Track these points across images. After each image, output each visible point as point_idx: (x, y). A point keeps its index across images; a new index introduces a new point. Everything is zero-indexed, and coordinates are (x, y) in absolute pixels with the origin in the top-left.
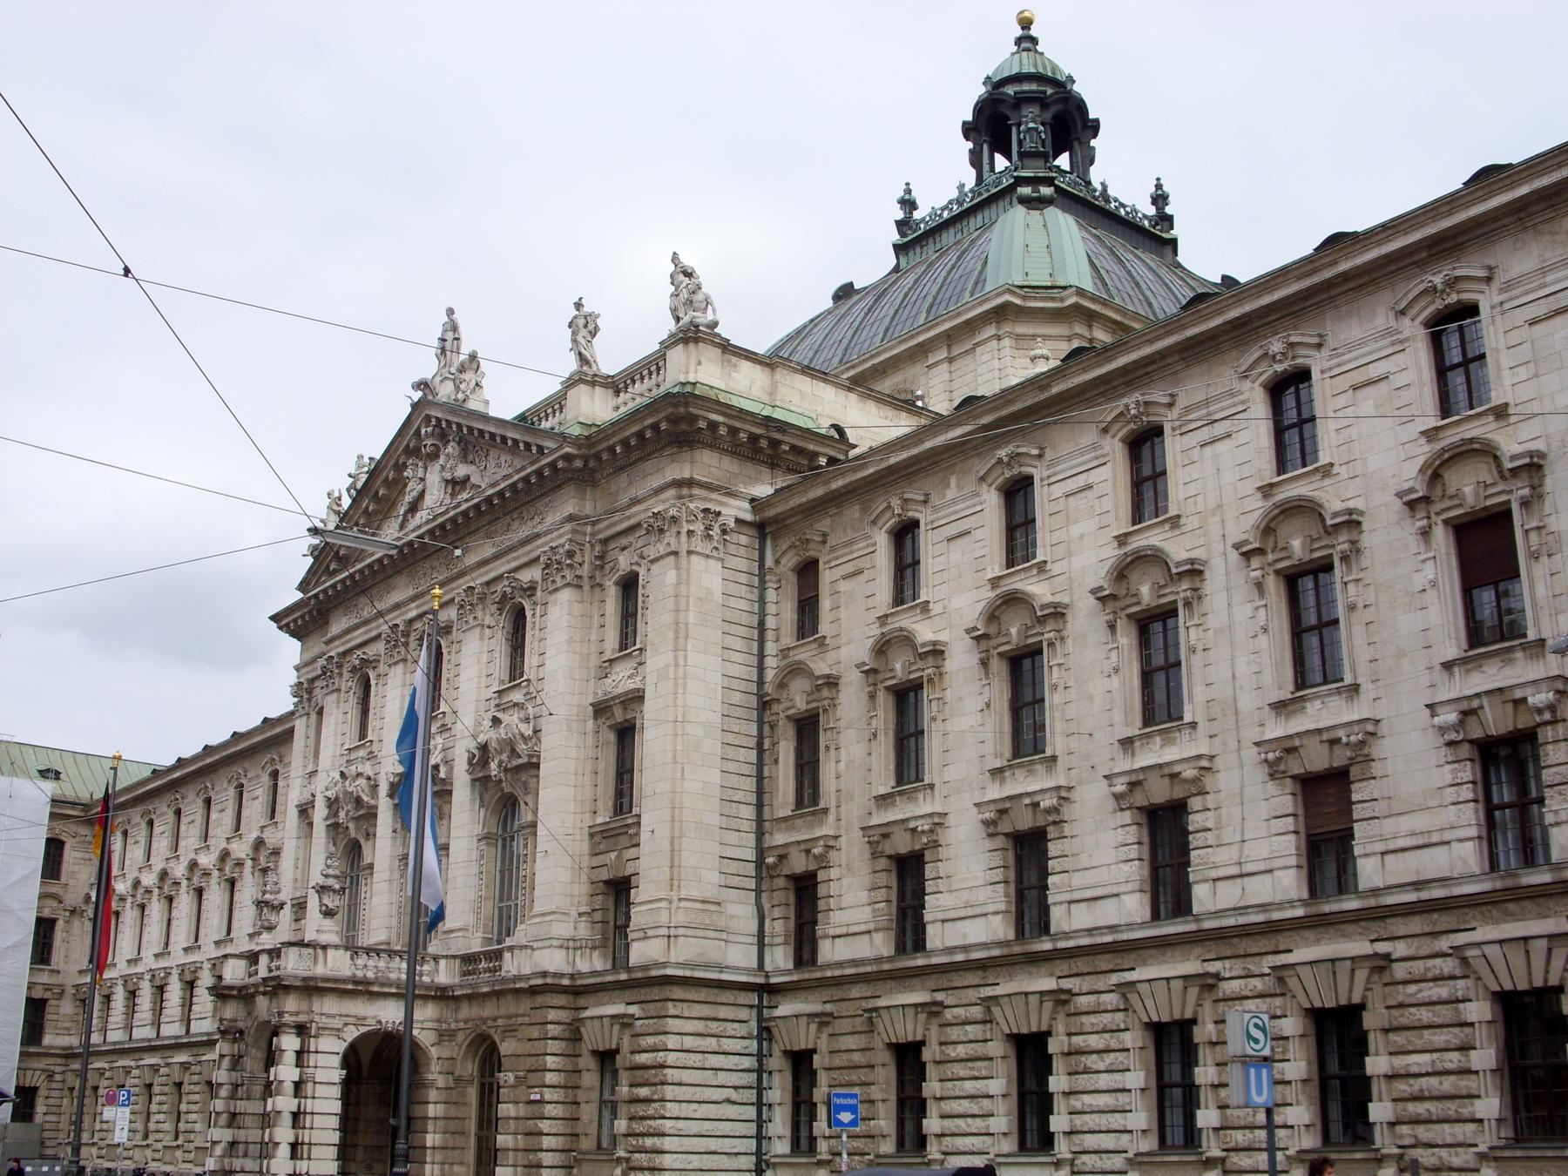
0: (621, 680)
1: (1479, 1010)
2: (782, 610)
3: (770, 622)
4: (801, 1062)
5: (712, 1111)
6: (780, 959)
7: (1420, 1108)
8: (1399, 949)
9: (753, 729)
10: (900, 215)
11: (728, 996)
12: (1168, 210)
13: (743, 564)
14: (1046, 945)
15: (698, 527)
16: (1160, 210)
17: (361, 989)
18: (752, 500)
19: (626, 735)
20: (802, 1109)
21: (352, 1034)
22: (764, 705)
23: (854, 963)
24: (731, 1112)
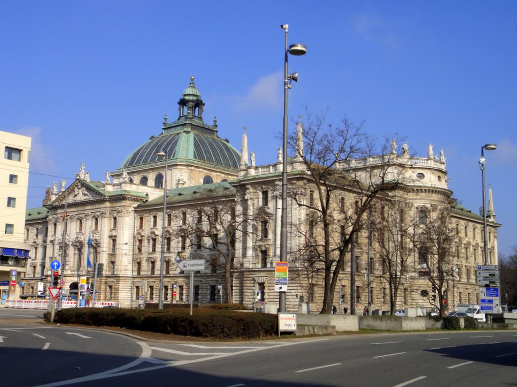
0: (114, 233)
1: (208, 287)
2: (138, 224)
3: (136, 225)
4: (137, 287)
5: (125, 294)
6: (135, 273)
7: (203, 297)
8: (203, 280)
9: (132, 241)
10: (163, 122)
11: (128, 278)
12: (217, 124)
13: (132, 217)
14: (168, 275)
15: (126, 212)
16: (215, 123)
17: (72, 276)
18: (134, 208)
19: (114, 241)
20: (138, 294)
21: (71, 283)
22: (134, 237)
23: (145, 275)
24: (127, 294)
